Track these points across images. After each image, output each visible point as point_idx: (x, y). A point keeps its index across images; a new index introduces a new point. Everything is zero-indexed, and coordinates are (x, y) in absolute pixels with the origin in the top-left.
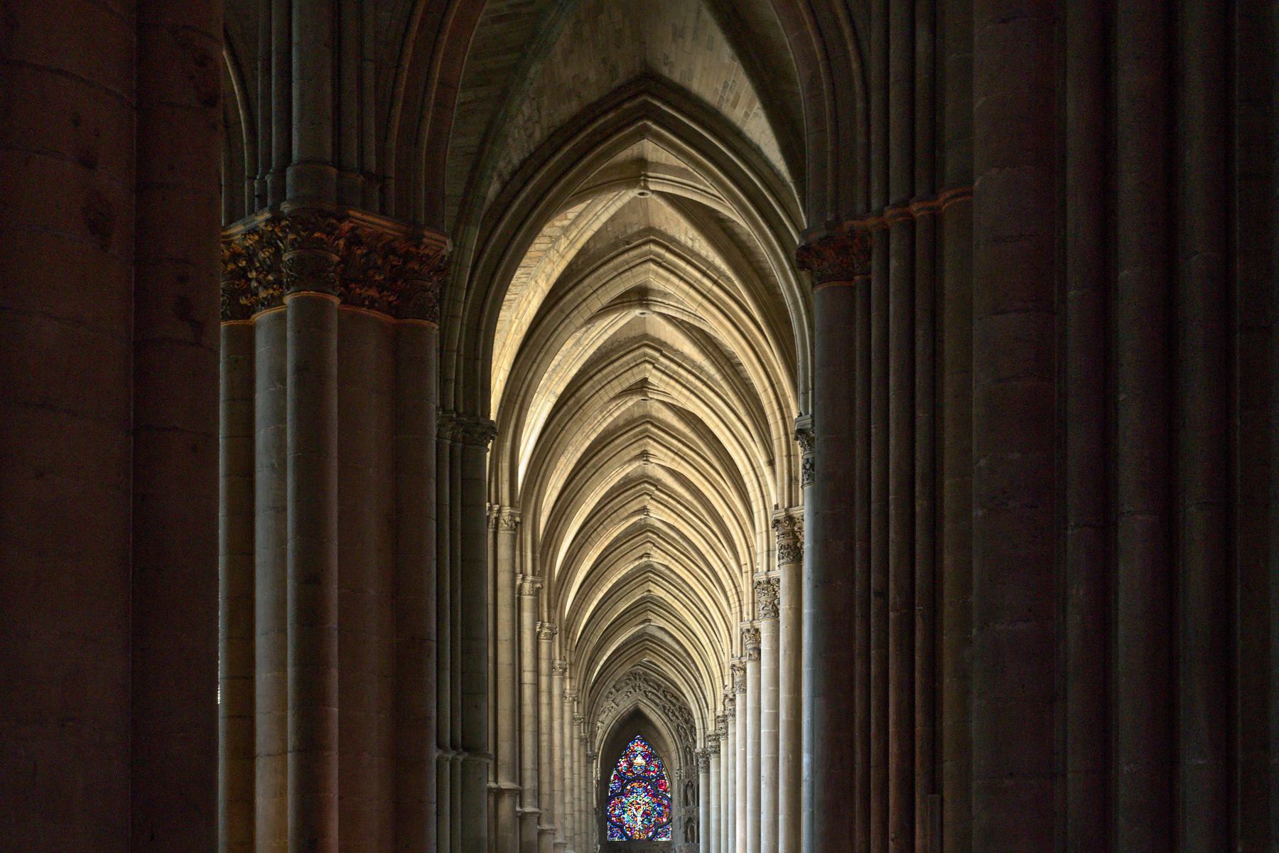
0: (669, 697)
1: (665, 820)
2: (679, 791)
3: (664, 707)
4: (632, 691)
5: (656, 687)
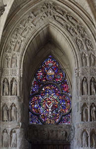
0: (70, 19)
1: (67, 111)
2: (77, 84)
3: (67, 27)
4: (45, 15)
5: (62, 13)
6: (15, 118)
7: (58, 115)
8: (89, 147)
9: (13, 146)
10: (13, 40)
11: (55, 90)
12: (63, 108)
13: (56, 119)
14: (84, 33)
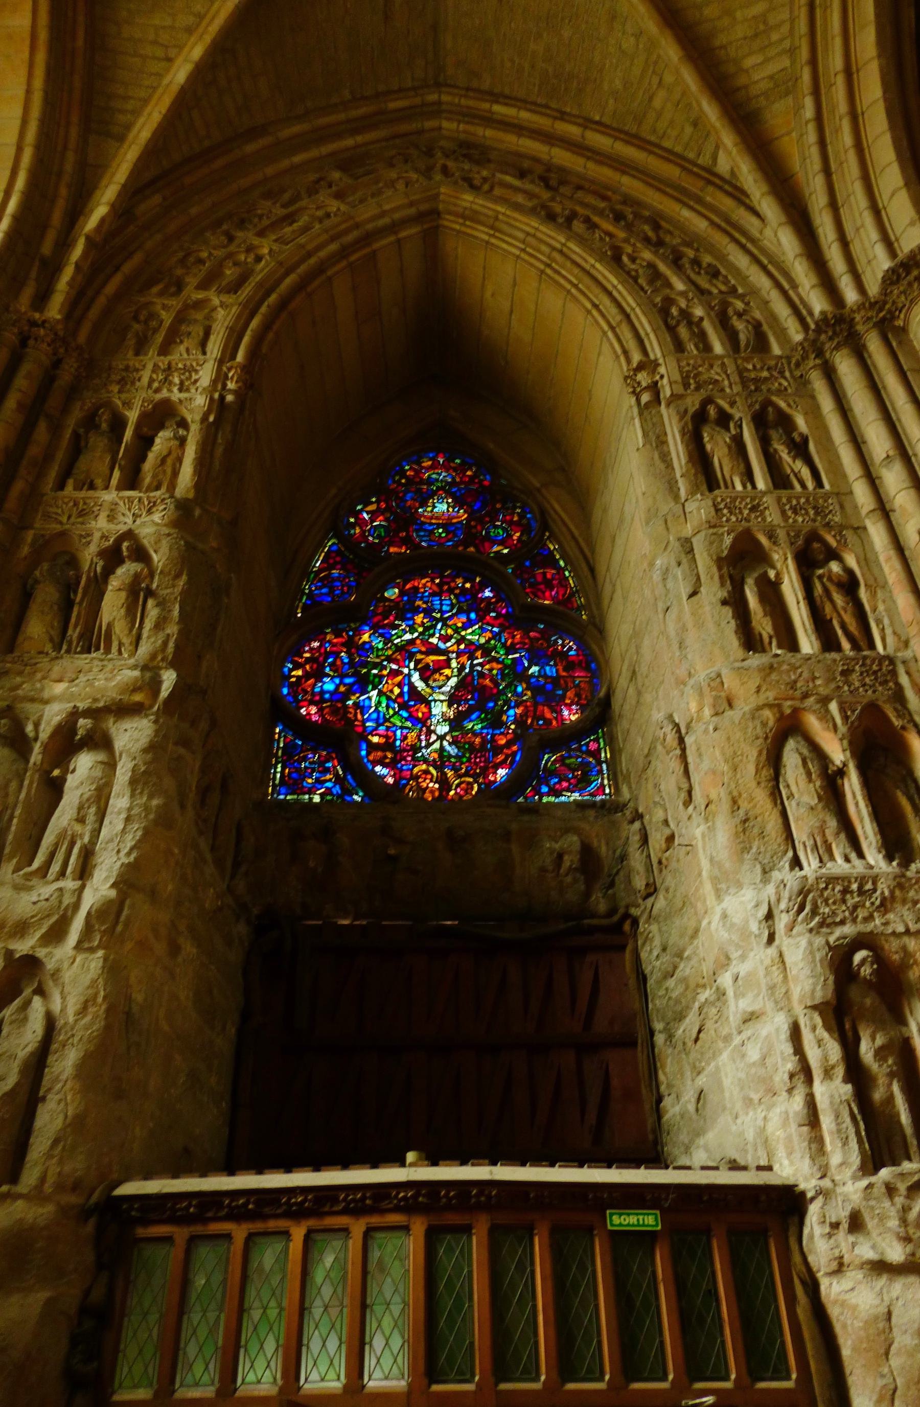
1: (571, 715)
6: (120, 629)
7: (503, 742)
9: (55, 868)
10: (204, 255)
12: (540, 699)
14: (658, 236)
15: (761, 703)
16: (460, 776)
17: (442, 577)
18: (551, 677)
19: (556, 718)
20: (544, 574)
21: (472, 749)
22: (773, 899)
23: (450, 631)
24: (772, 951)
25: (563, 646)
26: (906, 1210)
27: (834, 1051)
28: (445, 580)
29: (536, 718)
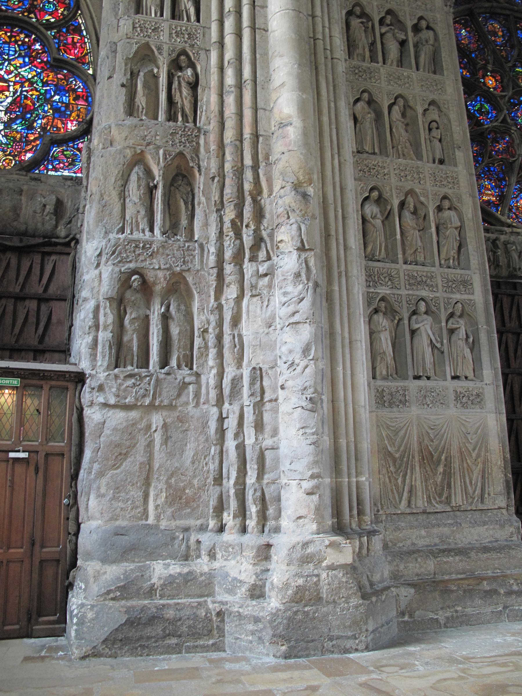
1: (72, 127)
7: (32, 138)
8: (157, 231)
11: (29, 47)
12: (56, 115)
13: (20, 152)
15: (126, 146)
16: (6, 155)
17: (11, 32)
18: (65, 103)
19: (63, 128)
20: (73, 38)
21: (14, 140)
22: (104, 247)
23: (12, 68)
24: (97, 272)
25: (75, 85)
26: (120, 385)
27: (110, 319)
28: (13, 34)
29: (52, 126)
